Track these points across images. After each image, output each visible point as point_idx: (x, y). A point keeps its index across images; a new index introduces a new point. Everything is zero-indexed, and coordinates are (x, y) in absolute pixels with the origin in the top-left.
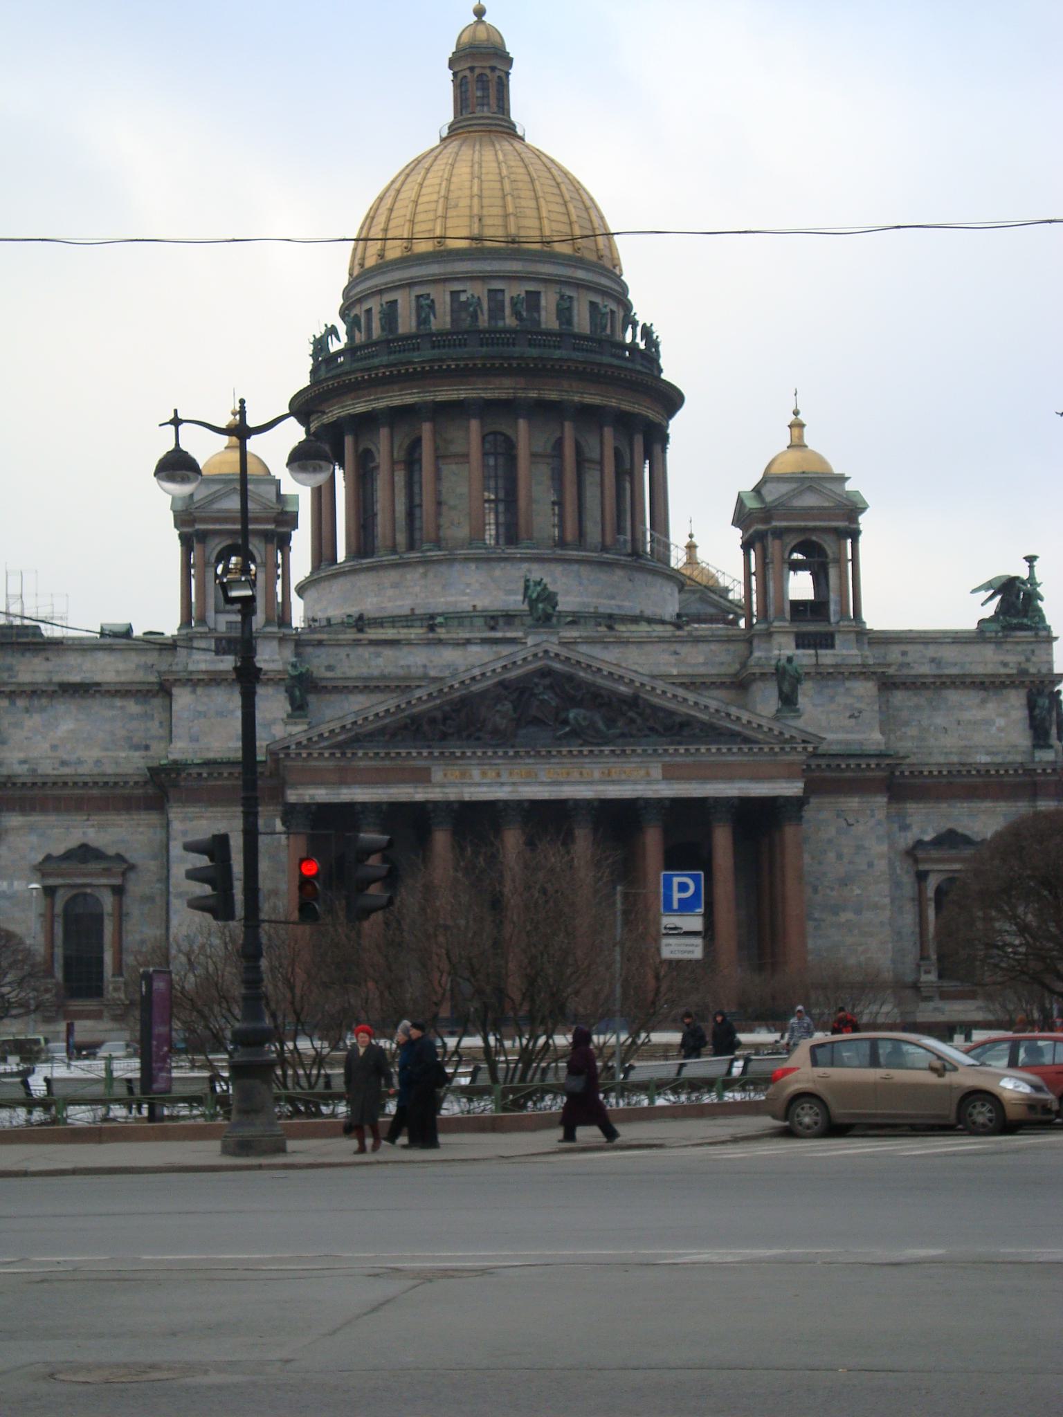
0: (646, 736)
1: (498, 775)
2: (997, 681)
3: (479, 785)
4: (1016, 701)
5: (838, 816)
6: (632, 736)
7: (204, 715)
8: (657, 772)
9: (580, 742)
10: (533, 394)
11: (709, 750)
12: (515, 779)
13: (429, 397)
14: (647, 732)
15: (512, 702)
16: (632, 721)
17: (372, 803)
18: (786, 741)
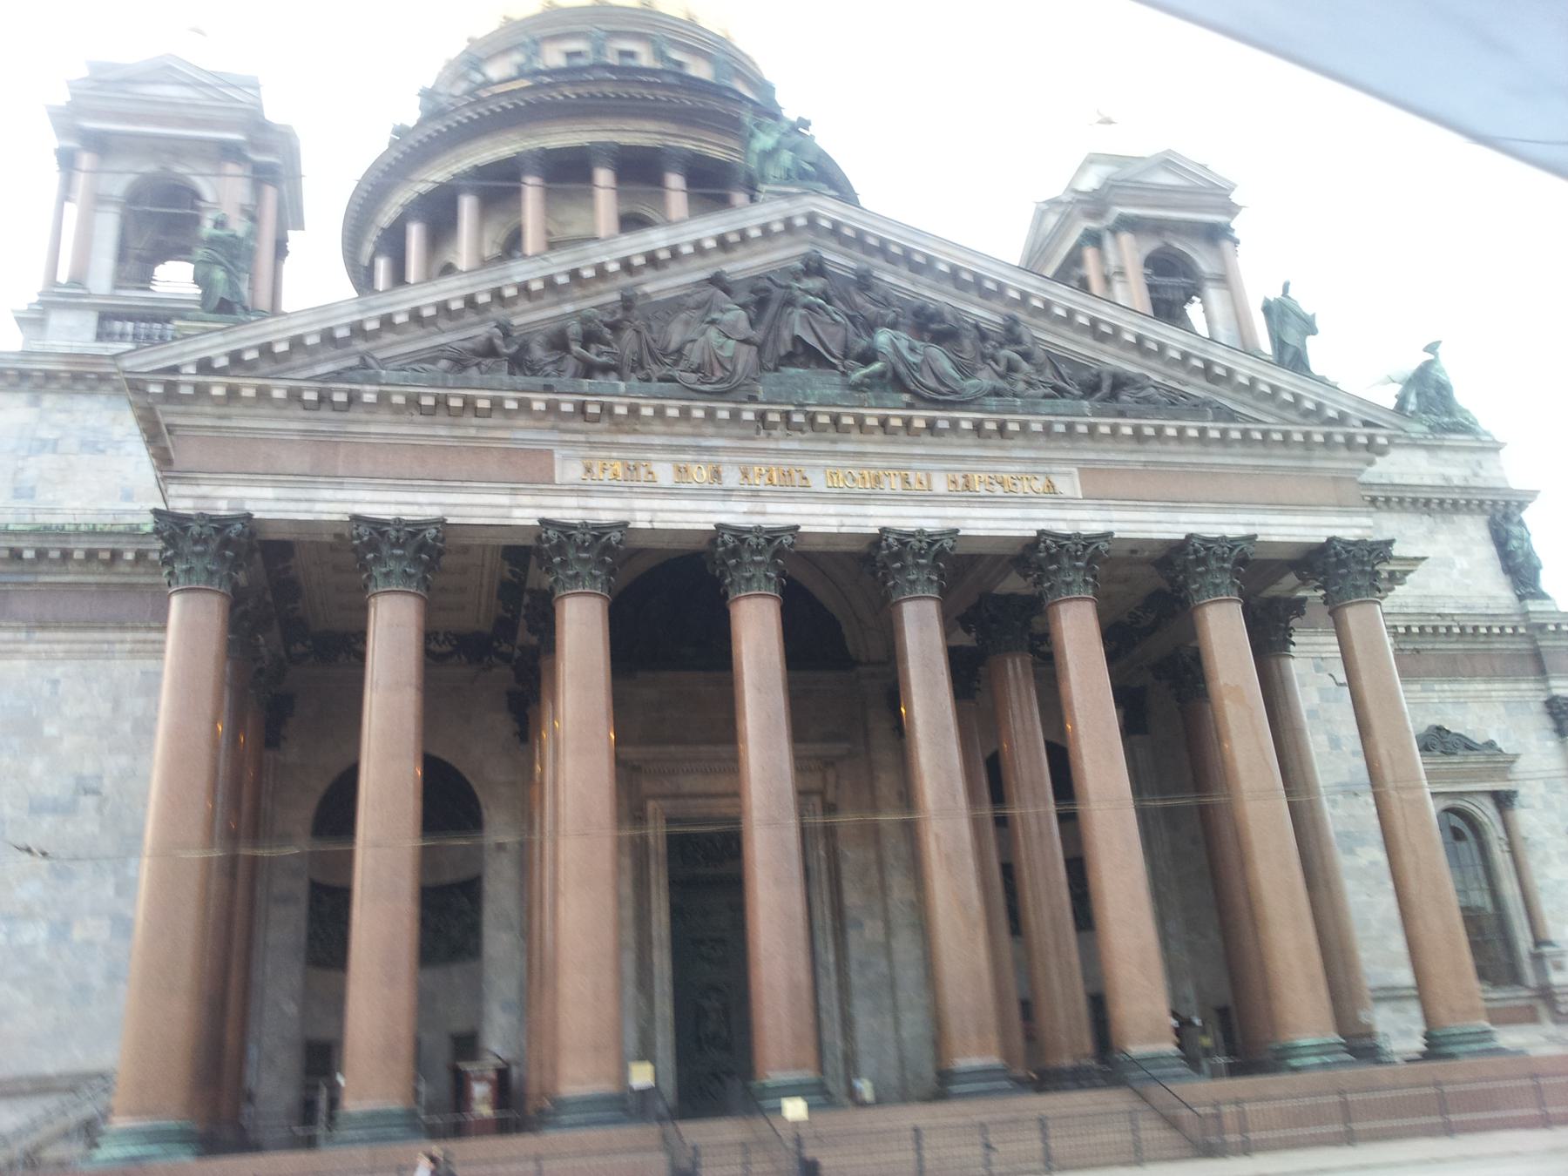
0: (1046, 396)
1: (716, 474)
2: (1448, 496)
3: (670, 493)
4: (1474, 530)
5: (1318, 669)
6: (1015, 395)
7: (53, 446)
8: (1070, 484)
9: (906, 397)
10: (688, 145)
11: (1181, 430)
12: (760, 483)
13: (533, 144)
14: (1049, 391)
15: (743, 306)
16: (1011, 368)
17: (399, 523)
18: (1331, 421)
